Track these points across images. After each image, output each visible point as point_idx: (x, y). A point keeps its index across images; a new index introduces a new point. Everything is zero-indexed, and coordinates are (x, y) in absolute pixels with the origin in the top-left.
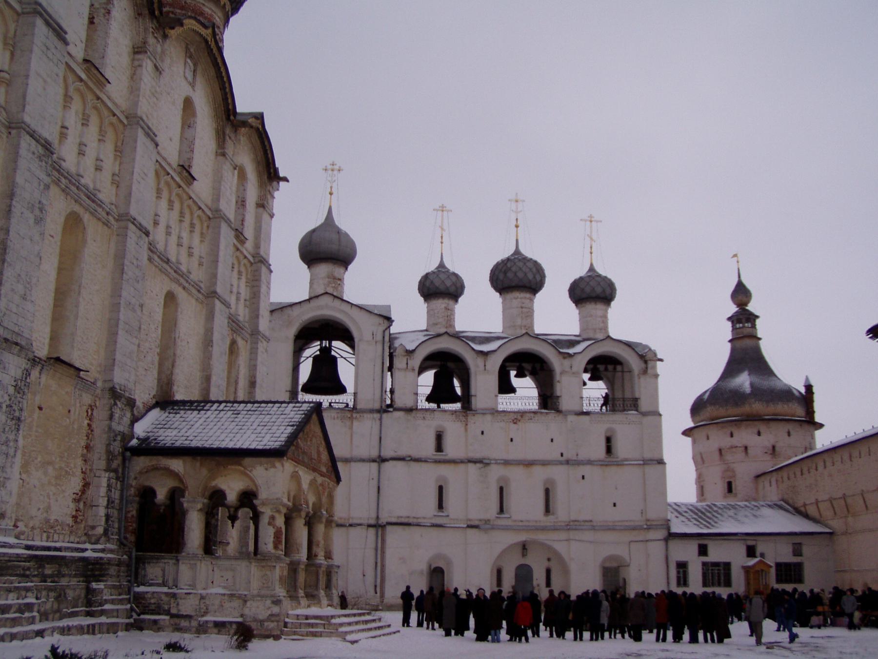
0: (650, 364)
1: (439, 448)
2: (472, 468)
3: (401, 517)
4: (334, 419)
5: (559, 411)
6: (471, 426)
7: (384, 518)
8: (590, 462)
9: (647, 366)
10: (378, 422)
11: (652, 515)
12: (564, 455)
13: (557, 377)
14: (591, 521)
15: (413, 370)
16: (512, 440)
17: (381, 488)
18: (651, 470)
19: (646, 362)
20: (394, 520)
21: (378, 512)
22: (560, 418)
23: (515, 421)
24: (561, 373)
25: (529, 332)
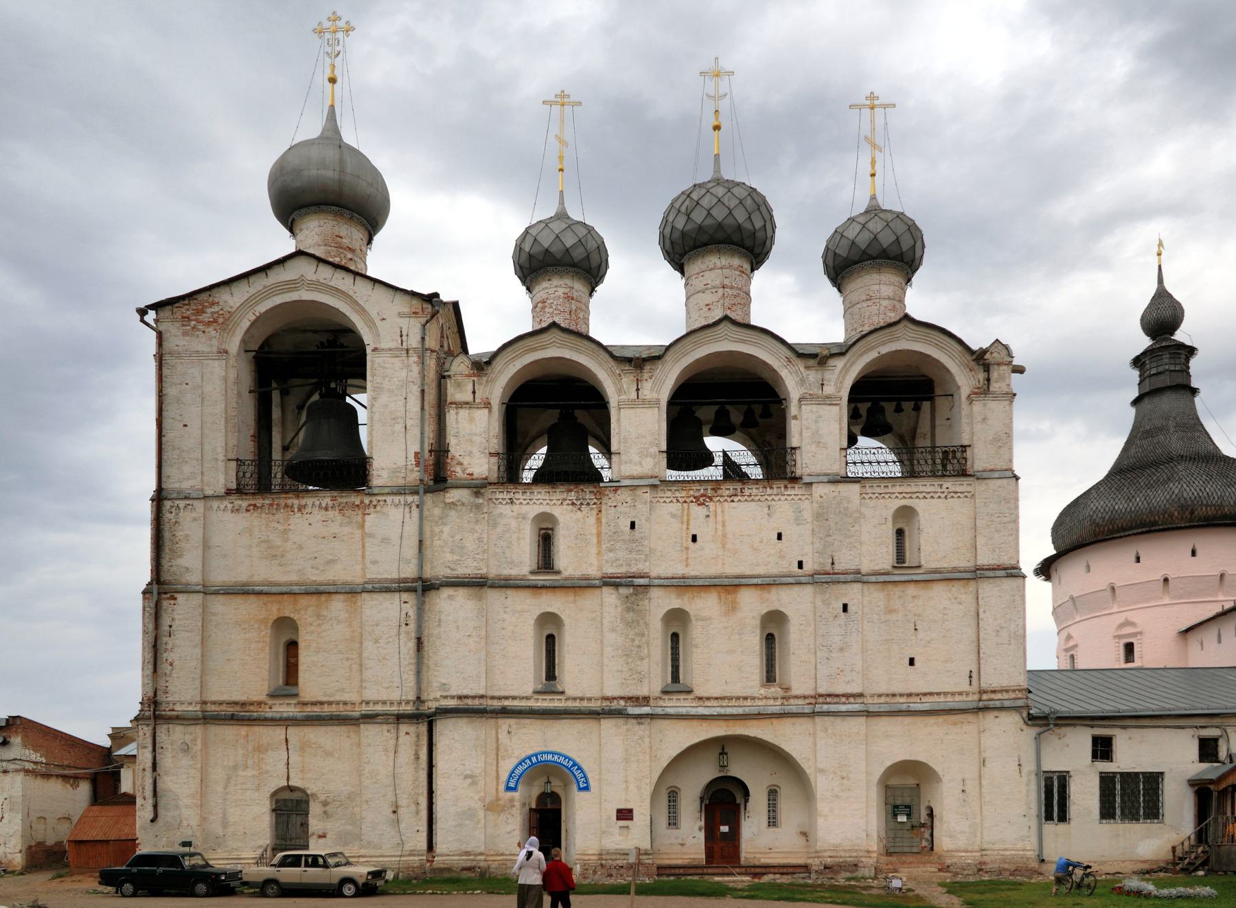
0: (994, 375)
1: (546, 562)
2: (610, 597)
3: (466, 697)
4: (326, 509)
5: (795, 479)
6: (608, 513)
7: (434, 699)
8: (857, 577)
9: (989, 375)
10: (415, 512)
11: (993, 678)
12: (804, 566)
13: (793, 409)
14: (861, 695)
15: (487, 405)
16: (694, 539)
17: (425, 639)
18: (991, 591)
19: (987, 368)
20: (452, 703)
21: (419, 689)
22: (797, 491)
23: (701, 499)
24: (800, 400)
25: (732, 315)
